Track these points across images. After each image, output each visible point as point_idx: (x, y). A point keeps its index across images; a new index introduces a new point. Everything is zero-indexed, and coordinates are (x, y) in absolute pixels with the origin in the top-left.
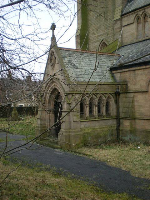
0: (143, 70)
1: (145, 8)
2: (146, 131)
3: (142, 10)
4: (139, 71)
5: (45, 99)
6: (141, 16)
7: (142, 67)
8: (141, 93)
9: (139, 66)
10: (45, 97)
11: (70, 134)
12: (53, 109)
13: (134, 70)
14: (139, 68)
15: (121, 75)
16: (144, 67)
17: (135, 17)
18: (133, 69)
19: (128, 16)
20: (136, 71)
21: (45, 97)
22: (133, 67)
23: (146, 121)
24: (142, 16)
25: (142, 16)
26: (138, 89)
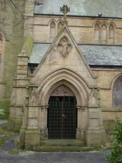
0: (106, 72)
1: (61, 17)
2: (108, 120)
3: (59, 18)
4: (103, 72)
5: (40, 92)
6: (57, 22)
7: (106, 69)
8: (104, 90)
9: (103, 68)
10: (41, 90)
11: (27, 132)
12: (48, 105)
13: (98, 71)
14: (103, 69)
15: (15, 68)
16: (109, 69)
17: (51, 20)
18: (97, 69)
19: (42, 17)
20: (99, 71)
21: (41, 90)
22: (97, 67)
23: (108, 112)
24: (58, 23)
25: (58, 23)
26: (101, 86)
